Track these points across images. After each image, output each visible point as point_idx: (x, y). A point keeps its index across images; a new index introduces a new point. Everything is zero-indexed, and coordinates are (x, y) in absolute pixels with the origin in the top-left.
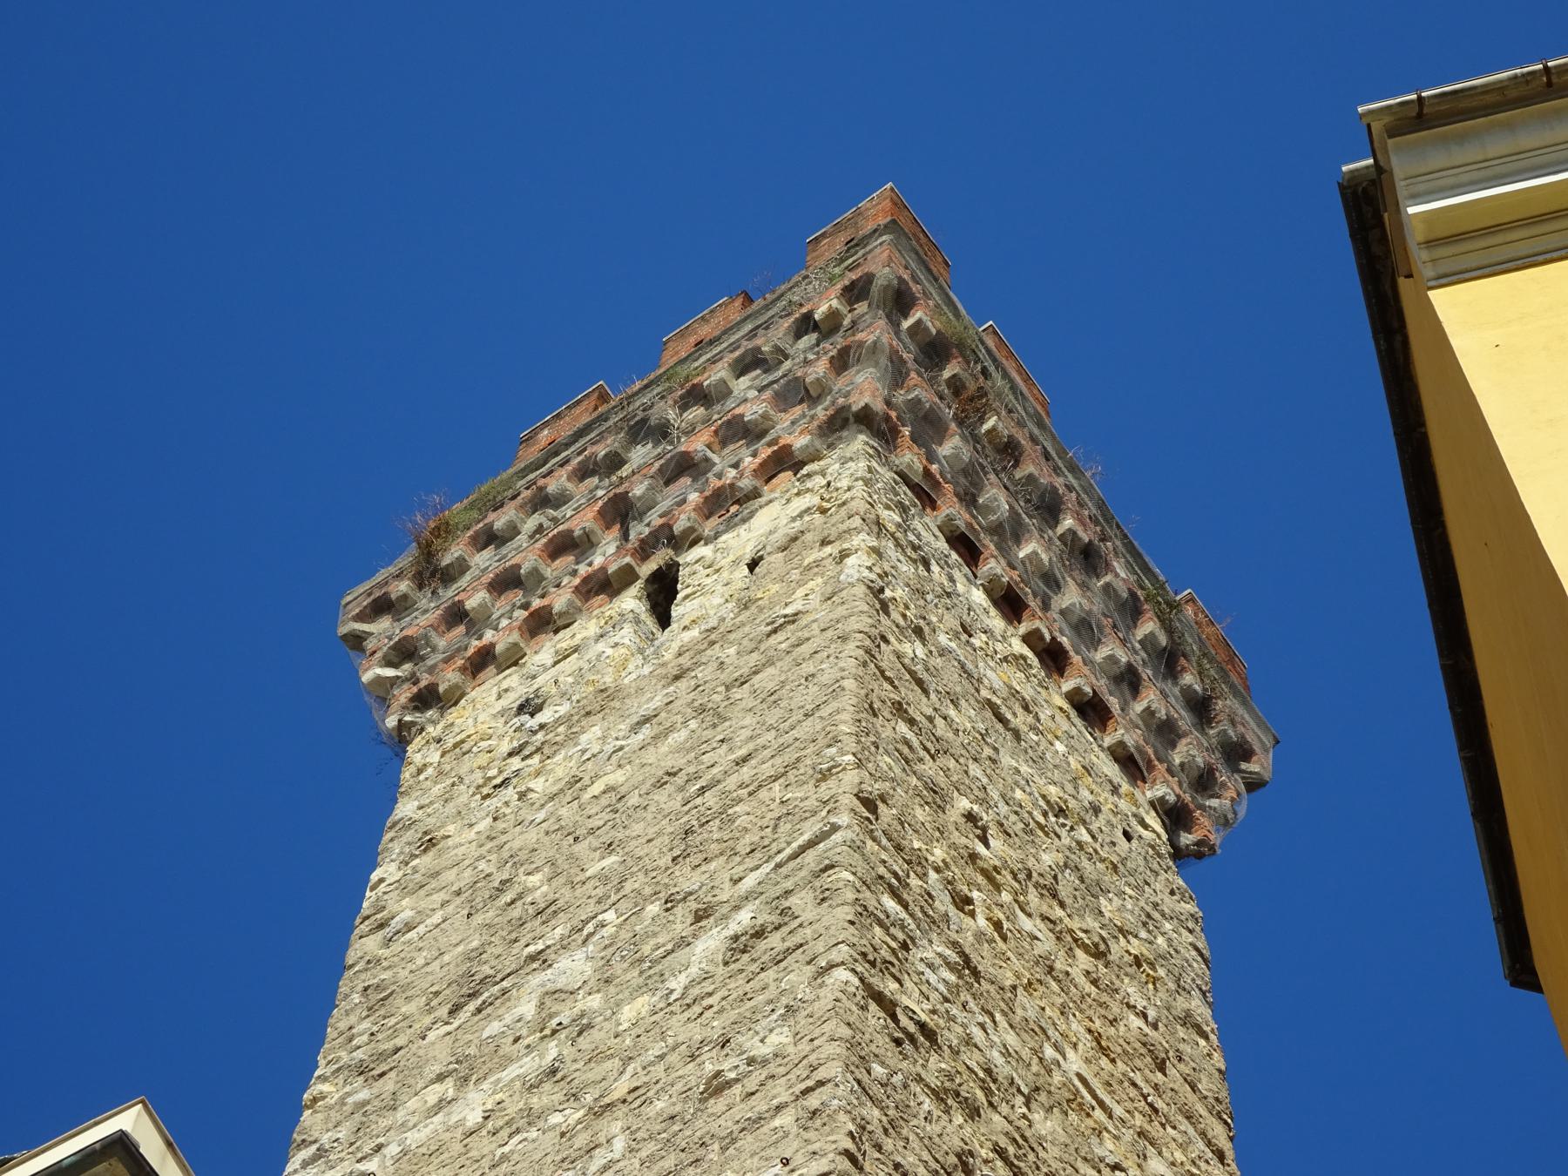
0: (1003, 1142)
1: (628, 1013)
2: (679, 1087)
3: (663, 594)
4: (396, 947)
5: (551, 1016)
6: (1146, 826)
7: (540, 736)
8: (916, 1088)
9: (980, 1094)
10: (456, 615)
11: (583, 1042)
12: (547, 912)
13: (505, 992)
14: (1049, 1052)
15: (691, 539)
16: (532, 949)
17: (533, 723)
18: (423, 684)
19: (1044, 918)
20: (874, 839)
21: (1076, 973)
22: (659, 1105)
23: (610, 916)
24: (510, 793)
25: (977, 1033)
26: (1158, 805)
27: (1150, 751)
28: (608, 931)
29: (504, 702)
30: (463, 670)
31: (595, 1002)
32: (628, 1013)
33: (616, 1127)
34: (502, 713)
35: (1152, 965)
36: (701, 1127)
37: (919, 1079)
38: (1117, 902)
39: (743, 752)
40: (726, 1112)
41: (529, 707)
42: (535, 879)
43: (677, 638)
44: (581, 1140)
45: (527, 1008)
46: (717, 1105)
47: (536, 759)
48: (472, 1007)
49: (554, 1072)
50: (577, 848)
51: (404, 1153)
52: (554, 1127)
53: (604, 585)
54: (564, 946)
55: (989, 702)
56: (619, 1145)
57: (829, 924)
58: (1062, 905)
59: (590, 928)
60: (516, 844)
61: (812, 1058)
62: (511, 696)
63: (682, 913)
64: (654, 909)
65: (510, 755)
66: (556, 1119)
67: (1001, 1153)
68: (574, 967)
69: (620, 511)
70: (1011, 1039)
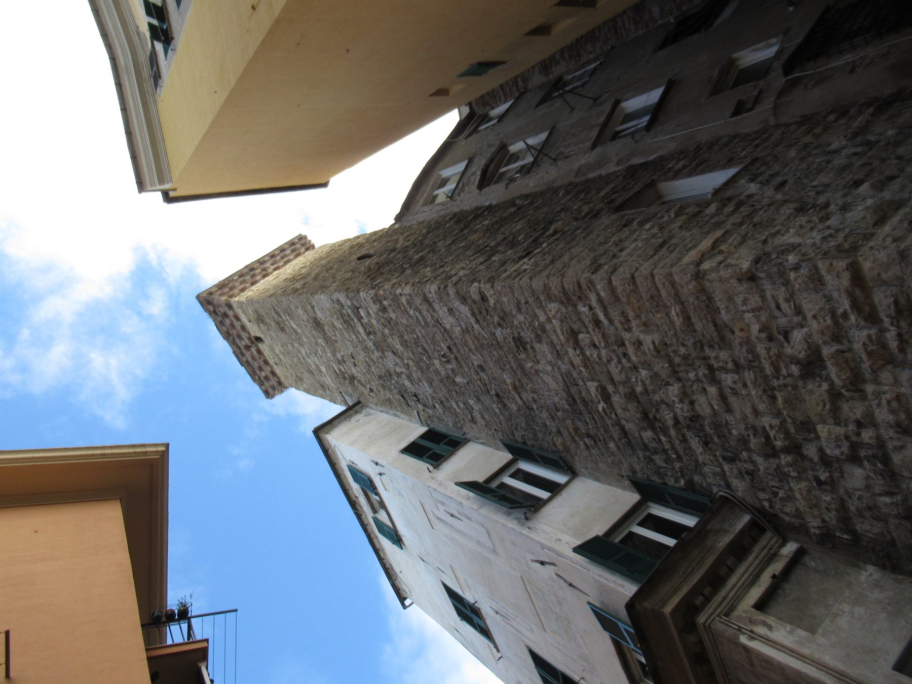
3: (259, 339)
10: (266, 378)
15: (249, 333)
43: (262, 336)
53: (259, 352)
69: (248, 348)
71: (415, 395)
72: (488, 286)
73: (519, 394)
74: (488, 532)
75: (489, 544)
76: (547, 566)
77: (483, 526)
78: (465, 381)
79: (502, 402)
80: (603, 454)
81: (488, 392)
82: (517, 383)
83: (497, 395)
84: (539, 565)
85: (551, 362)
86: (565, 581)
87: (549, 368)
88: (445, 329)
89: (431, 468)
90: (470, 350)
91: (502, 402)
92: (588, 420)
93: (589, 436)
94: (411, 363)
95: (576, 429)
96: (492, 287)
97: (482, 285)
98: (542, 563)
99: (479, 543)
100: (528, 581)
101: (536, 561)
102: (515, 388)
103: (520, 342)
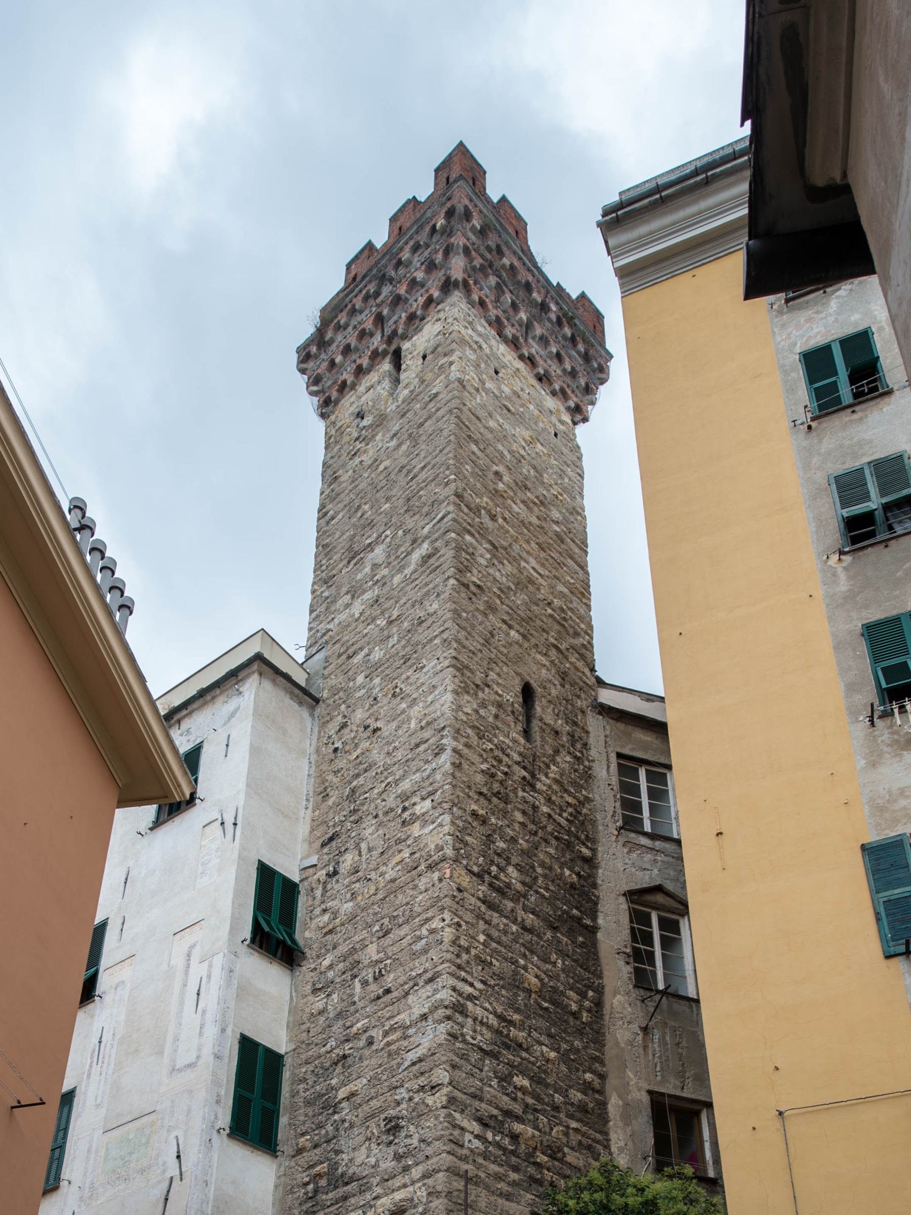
0: (506, 618)
1: (397, 579)
2: (410, 618)
4: (330, 527)
5: (375, 575)
6: (562, 422)
7: (364, 432)
8: (476, 614)
9: (498, 601)
11: (386, 589)
12: (371, 524)
13: (362, 558)
14: (523, 564)
16: (369, 541)
17: (361, 425)
18: (327, 394)
19: (523, 502)
20: (462, 511)
21: (534, 520)
22: (406, 624)
23: (388, 532)
24: (357, 460)
25: (497, 574)
26: (568, 409)
27: (565, 386)
28: (388, 540)
29: (352, 409)
30: (338, 391)
31: (385, 572)
32: (397, 579)
33: (395, 630)
34: (352, 414)
35: (561, 495)
36: (416, 638)
37: (477, 609)
38: (550, 471)
39: (422, 464)
40: (421, 635)
41: (360, 415)
42: (366, 507)
44: (386, 633)
45: (368, 569)
46: (420, 630)
47: (363, 445)
48: (353, 562)
49: (377, 601)
50: (378, 495)
51: (340, 623)
52: (378, 625)
54: (377, 542)
55: (504, 406)
56: (396, 638)
57: (448, 554)
58: (529, 490)
59: (383, 536)
60: (360, 487)
61: (444, 618)
62: (355, 406)
63: (409, 537)
64: (400, 533)
65: (357, 439)
66: (378, 622)
67: (504, 622)
68: (379, 553)
70: (509, 568)
71: (335, 873)
72: (444, 1099)
73: (348, 1098)
74: (191, 1065)
75: (179, 1065)
76: (177, 1161)
77: (198, 1057)
78: (356, 999)
79: (339, 1061)
80: (300, 1204)
81: (347, 1040)
82: (358, 1100)
83: (345, 1057)
84: (176, 1154)
85: (379, 1166)
86: (168, 1191)
87: (373, 1160)
88: (407, 994)
89: (248, 942)
90: (386, 1034)
91: (339, 1061)
92: (330, 1195)
93: (316, 1191)
94: (373, 889)
95: (319, 1175)
96: (443, 1107)
97: (445, 1090)
98: (178, 1157)
99: (176, 1039)
100: (153, 1124)
101: (178, 1145)
102: (353, 1094)
103: (393, 1128)
